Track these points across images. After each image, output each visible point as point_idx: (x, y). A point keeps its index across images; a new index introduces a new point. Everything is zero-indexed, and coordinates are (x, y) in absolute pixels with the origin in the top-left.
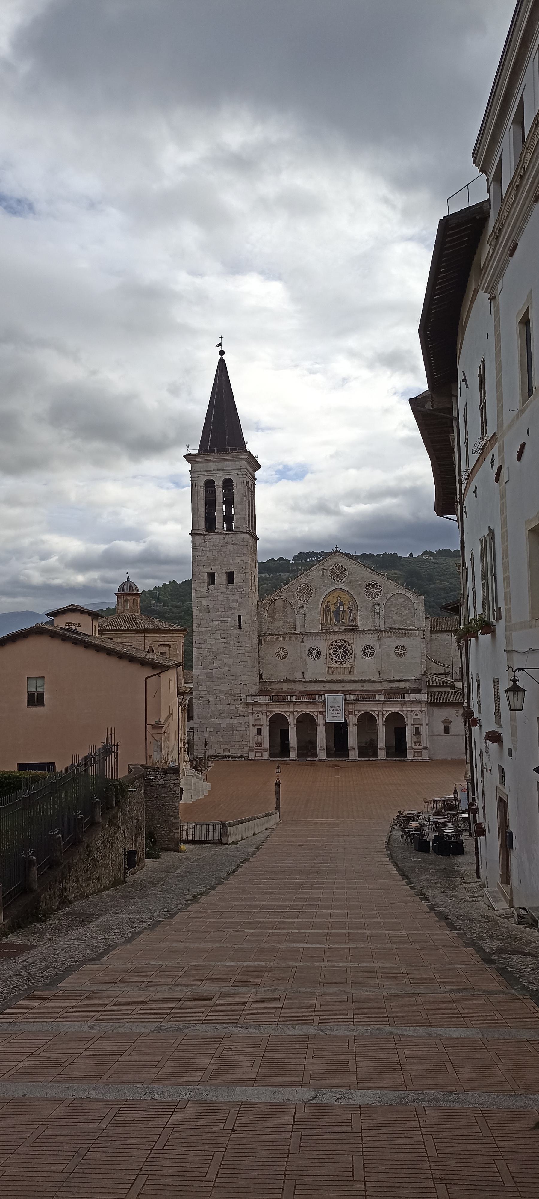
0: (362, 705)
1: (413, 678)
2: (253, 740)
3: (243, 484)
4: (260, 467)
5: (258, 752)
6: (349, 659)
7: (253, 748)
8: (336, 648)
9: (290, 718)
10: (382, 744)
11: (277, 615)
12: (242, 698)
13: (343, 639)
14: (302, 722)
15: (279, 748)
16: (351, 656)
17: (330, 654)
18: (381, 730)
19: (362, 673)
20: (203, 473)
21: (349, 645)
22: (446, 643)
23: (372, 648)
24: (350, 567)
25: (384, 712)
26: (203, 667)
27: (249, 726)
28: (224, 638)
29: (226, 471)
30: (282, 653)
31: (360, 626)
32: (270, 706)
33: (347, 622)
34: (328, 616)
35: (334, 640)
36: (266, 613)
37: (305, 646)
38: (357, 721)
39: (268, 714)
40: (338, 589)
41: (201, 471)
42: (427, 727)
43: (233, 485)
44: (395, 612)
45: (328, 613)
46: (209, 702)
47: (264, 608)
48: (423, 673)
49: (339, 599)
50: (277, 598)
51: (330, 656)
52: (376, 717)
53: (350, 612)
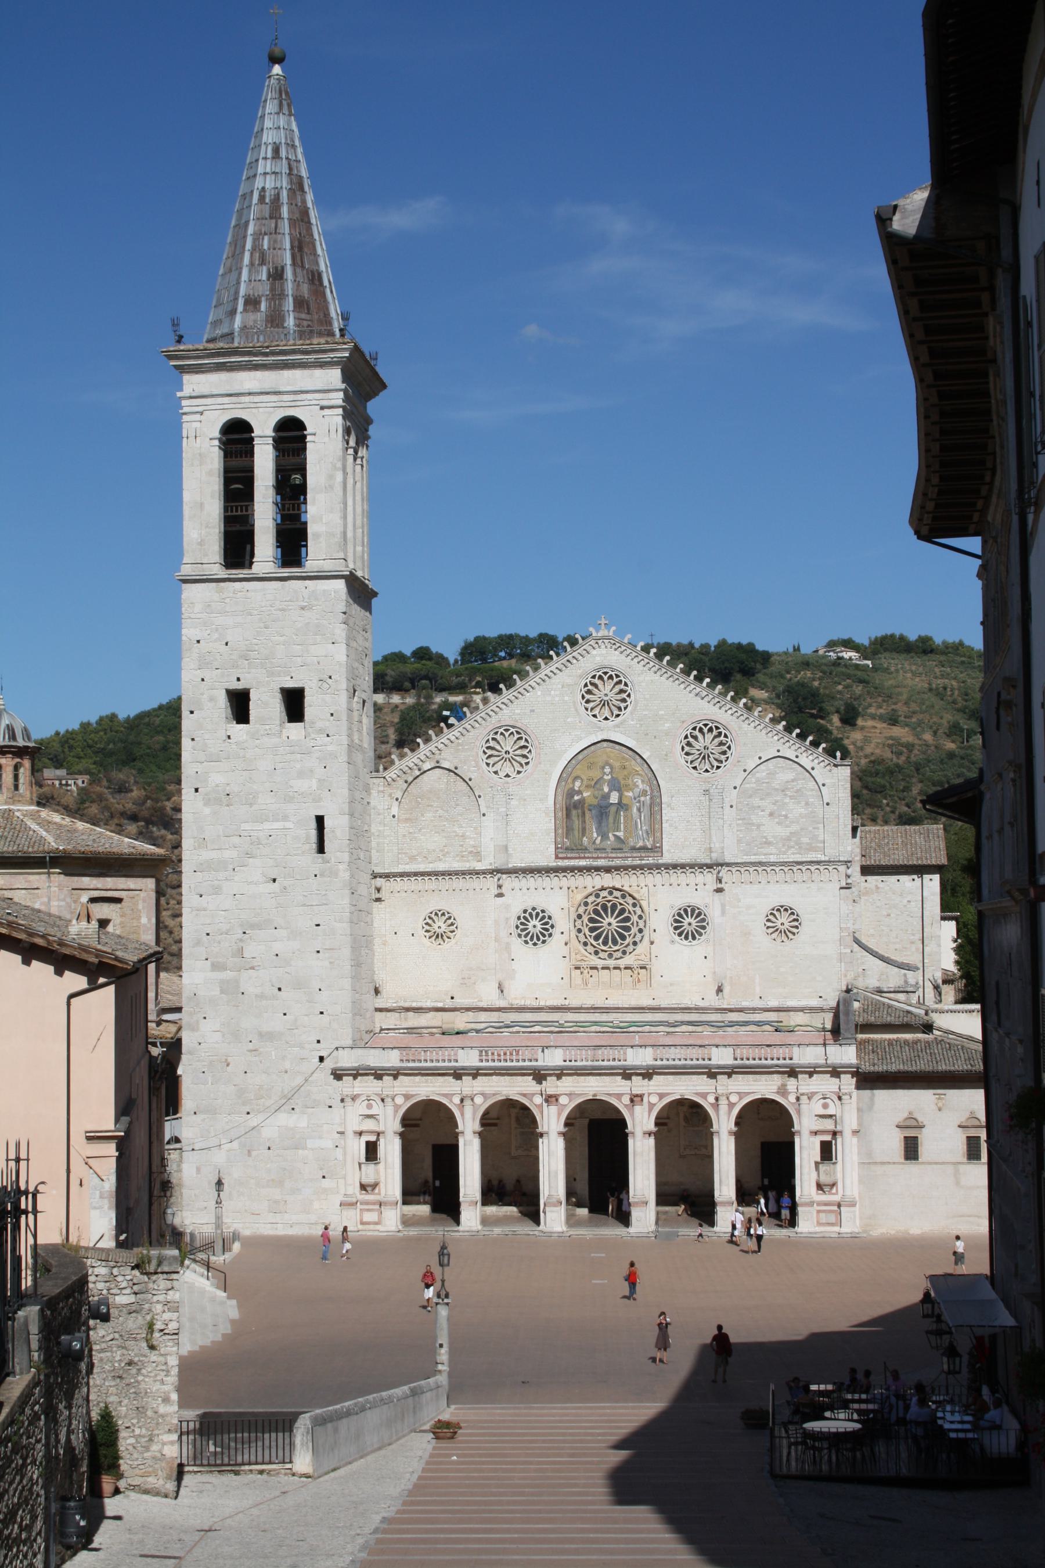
0: (671, 1078)
1: (815, 1003)
3: (333, 431)
4: (384, 386)
5: (368, 1210)
6: (635, 943)
7: (354, 1200)
8: (596, 912)
9: (462, 1114)
10: (725, 1187)
11: (429, 815)
13: (618, 886)
14: (495, 1125)
16: (639, 936)
17: (579, 931)
18: (724, 1149)
19: (671, 985)
20: (220, 400)
21: (634, 905)
22: (905, 901)
23: (699, 914)
24: (641, 678)
25: (734, 1099)
26: (213, 965)
28: (274, 880)
29: (286, 397)
30: (440, 925)
31: (668, 851)
33: (631, 842)
34: (574, 818)
35: (590, 890)
36: (395, 810)
37: (507, 907)
38: (657, 1124)
39: (399, 1100)
40: (605, 744)
41: (213, 396)
42: (855, 1140)
43: (305, 437)
44: (767, 812)
45: (574, 812)
46: (228, 1065)
47: (390, 795)
48: (844, 988)
49: (607, 770)
50: (427, 766)
51: (581, 935)
52: (711, 1111)
53: (639, 810)
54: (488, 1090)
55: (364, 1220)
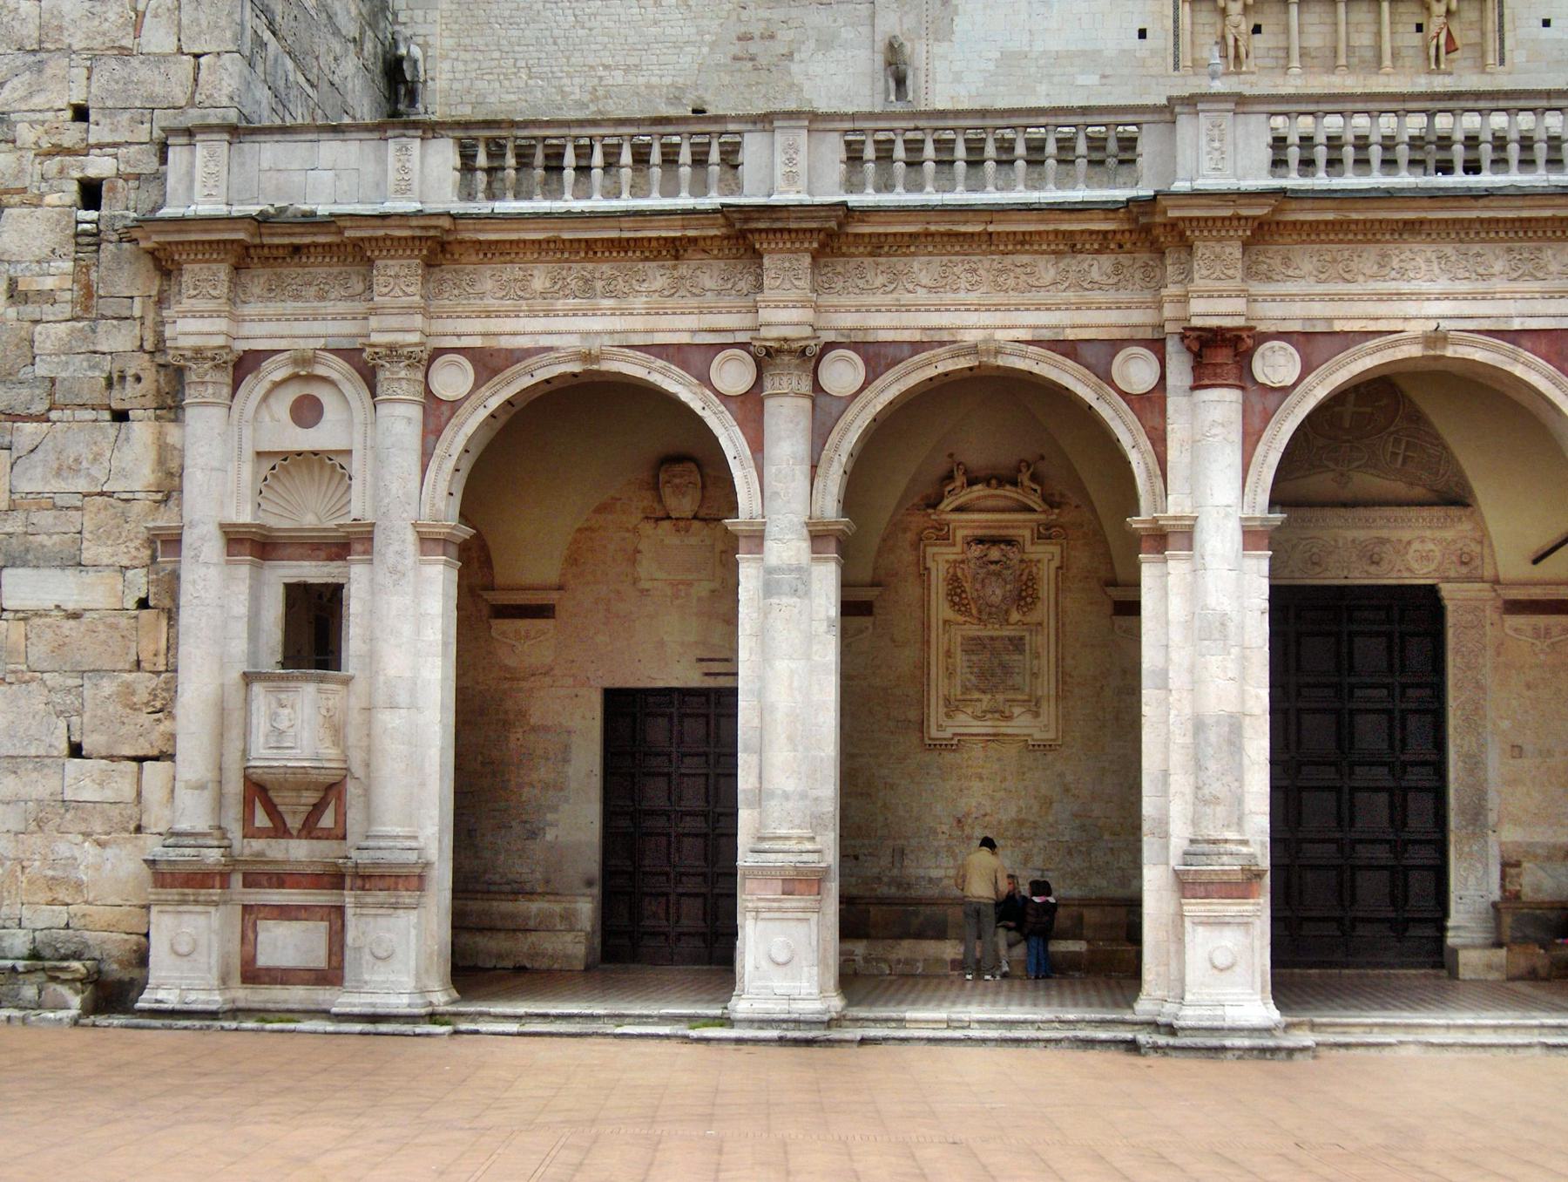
2: (221, 735)
5: (285, 913)
7: (213, 856)
9: (757, 445)
12: (100, 166)
15: (586, 909)
27: (168, 542)
32: (489, 280)
39: (452, 380)
54: (886, 325)
55: (263, 961)
